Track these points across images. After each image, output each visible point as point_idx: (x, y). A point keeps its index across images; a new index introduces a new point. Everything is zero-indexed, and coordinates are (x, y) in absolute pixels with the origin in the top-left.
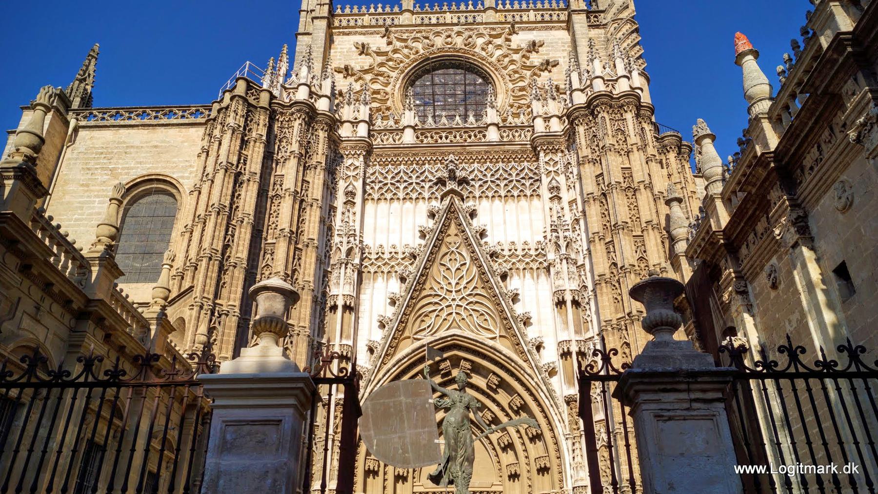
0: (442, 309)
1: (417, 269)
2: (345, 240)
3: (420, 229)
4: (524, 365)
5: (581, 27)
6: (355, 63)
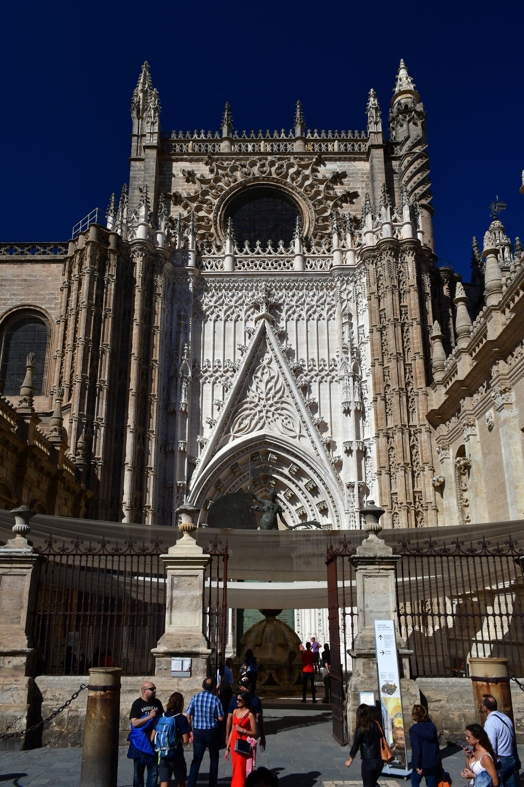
3: (238, 347)
5: (379, 161)
6: (182, 189)
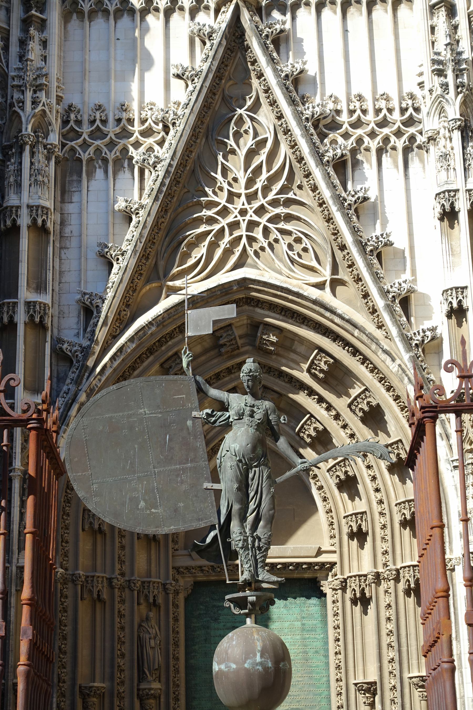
0: (222, 230)
1: (171, 152)
2: (29, 95)
4: (379, 334)
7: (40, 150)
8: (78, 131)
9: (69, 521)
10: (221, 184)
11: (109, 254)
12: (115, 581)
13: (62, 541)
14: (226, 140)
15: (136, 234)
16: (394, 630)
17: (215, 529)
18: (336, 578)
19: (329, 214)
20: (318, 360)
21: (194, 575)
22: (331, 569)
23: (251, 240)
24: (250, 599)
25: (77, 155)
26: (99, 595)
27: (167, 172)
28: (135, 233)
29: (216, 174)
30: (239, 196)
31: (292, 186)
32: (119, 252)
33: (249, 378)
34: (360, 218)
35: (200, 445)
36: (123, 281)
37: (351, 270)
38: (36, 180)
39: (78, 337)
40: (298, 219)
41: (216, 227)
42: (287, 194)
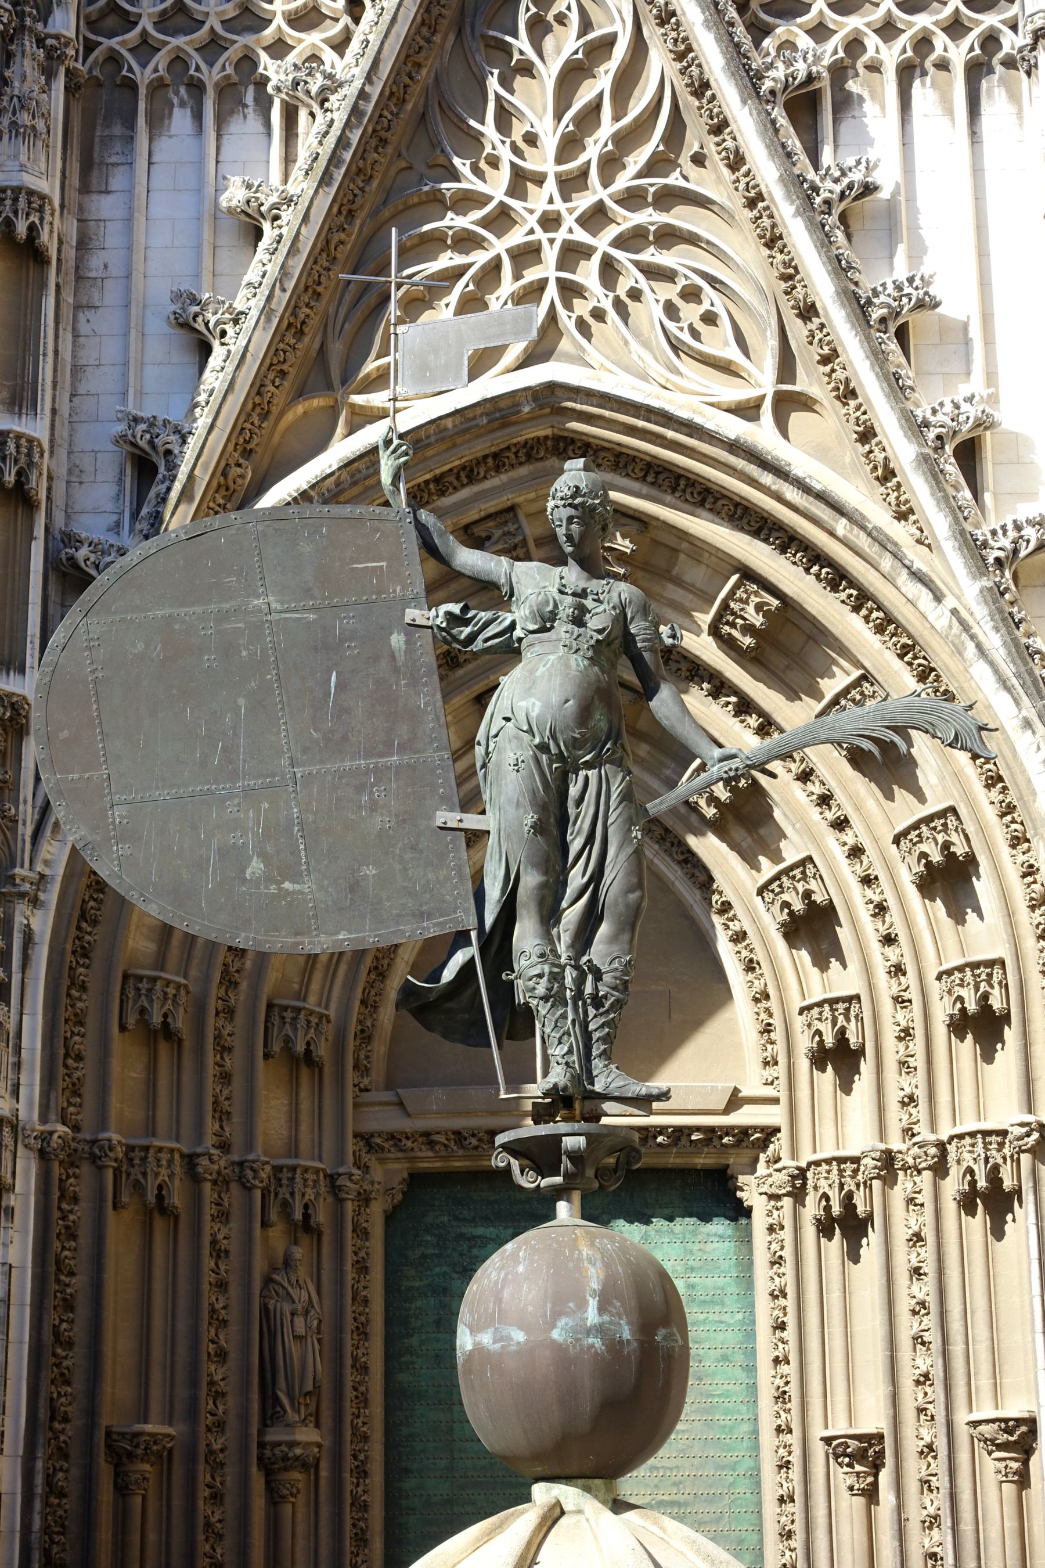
0: (494, 267)
1: (366, 63)
4: (900, 533)
7: (28, 48)
8: (127, 12)
9: (87, 1003)
10: (494, 148)
11: (200, 319)
12: (204, 1161)
13: (67, 1055)
14: (509, 39)
15: (273, 270)
16: (932, 1302)
17: (469, 943)
18: (778, 1166)
19: (774, 226)
20: (741, 600)
21: (411, 1154)
22: (764, 1144)
23: (570, 291)
24: (569, 1142)
25: (124, 73)
26: (160, 1197)
27: (355, 111)
28: (268, 268)
29: (483, 123)
30: (539, 180)
31: (678, 156)
32: (227, 316)
33: (571, 511)
34: (854, 239)
35: (426, 704)
36: (237, 387)
37: (828, 369)
38: (13, 124)
39: (118, 533)
40: (692, 239)
41: (480, 258)
42: (666, 176)
